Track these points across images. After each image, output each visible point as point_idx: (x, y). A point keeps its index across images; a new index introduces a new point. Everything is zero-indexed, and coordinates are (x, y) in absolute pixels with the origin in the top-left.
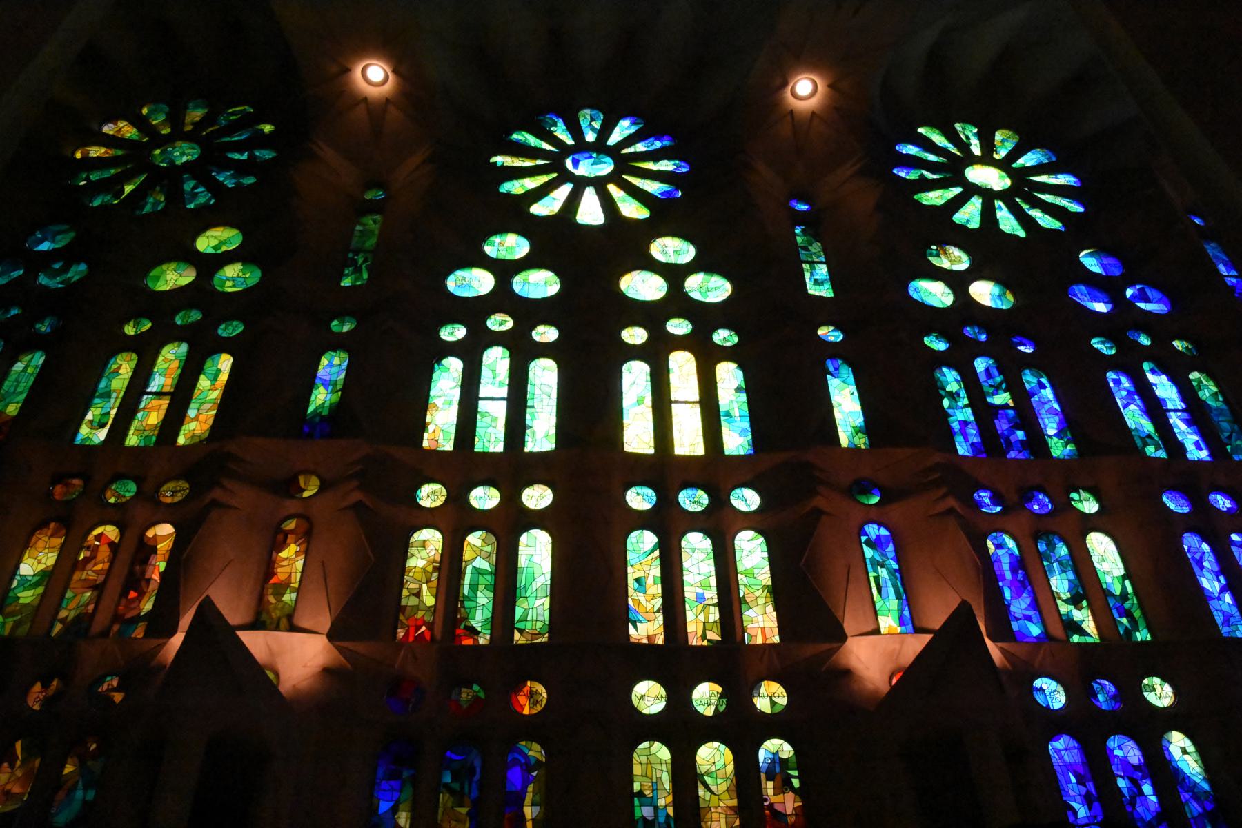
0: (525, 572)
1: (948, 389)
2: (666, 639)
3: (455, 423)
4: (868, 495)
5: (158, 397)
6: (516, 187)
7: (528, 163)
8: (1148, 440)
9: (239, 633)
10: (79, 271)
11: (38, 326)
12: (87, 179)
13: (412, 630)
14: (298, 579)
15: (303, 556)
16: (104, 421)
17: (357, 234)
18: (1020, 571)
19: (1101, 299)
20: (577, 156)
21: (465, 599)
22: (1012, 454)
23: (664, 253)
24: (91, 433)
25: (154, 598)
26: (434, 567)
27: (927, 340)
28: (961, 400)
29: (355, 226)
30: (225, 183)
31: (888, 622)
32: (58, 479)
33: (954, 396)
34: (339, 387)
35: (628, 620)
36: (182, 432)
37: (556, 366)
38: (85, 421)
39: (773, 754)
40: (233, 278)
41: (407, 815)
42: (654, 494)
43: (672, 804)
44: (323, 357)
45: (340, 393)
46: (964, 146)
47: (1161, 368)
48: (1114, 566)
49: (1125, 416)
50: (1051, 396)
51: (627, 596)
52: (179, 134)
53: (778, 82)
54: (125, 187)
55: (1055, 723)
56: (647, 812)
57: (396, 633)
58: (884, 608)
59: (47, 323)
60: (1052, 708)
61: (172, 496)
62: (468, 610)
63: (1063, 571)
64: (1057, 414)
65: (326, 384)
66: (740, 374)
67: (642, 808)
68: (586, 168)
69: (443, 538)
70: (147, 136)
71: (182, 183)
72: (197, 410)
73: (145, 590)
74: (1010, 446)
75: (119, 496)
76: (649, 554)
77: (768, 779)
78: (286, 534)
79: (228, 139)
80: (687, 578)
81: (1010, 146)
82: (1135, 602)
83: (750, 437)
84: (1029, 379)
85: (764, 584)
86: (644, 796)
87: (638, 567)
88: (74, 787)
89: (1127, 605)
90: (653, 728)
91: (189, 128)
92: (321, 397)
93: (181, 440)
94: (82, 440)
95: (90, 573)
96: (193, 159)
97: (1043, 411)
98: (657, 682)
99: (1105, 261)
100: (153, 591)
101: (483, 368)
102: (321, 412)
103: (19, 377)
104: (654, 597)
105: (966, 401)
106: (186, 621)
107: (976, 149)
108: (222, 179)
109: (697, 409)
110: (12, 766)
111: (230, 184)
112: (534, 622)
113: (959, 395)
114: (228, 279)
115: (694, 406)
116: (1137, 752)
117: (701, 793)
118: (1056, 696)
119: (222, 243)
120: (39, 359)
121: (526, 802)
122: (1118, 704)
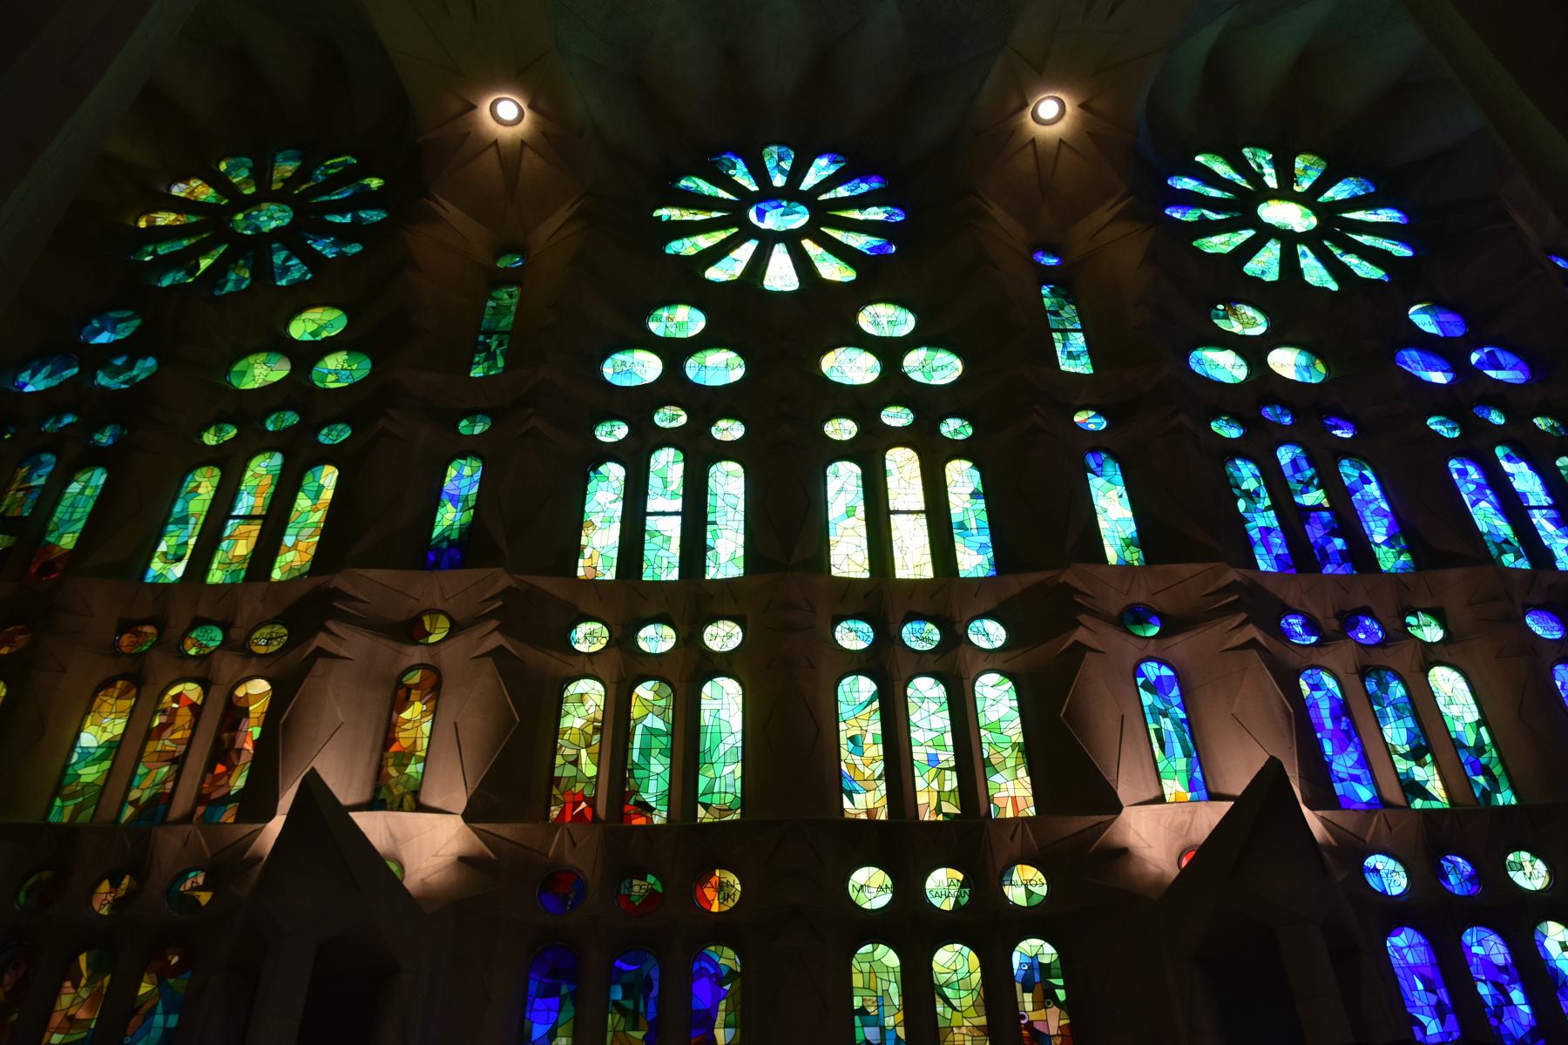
0: (709, 731)
1: (1244, 486)
2: (890, 814)
3: (617, 545)
4: (1145, 625)
5: (246, 522)
6: (687, 247)
7: (701, 216)
8: (1505, 546)
9: (352, 815)
10: (146, 366)
11: (97, 437)
12: (154, 253)
13: (568, 810)
14: (425, 746)
15: (431, 717)
16: (180, 552)
17: (489, 311)
18: (1343, 719)
19: (1438, 368)
20: (762, 206)
21: (635, 766)
22: (1329, 569)
23: (876, 324)
24: (165, 569)
25: (245, 774)
26: (595, 728)
27: (1214, 426)
28: (1262, 500)
29: (487, 301)
30: (324, 253)
31: (1175, 787)
32: (127, 626)
33: (1251, 496)
34: (471, 503)
35: (841, 791)
36: (277, 565)
37: (742, 470)
38: (157, 554)
39: (1031, 957)
40: (336, 370)
41: (567, 1041)
42: (870, 630)
43: (902, 1024)
44: (450, 467)
45: (472, 511)
46: (1256, 177)
47: (1521, 452)
48: (1466, 709)
49: (1474, 516)
50: (1377, 493)
51: (839, 760)
52: (265, 195)
53: (1015, 103)
54: (201, 261)
55: (1395, 913)
56: (872, 1033)
57: (548, 811)
58: (1169, 769)
59: (108, 432)
60: (1390, 894)
61: (267, 644)
62: (639, 781)
63: (1399, 718)
64: (1386, 516)
65: (454, 500)
66: (976, 474)
67: (865, 1028)
68: (774, 220)
69: (606, 691)
70: (226, 198)
71: (271, 253)
72: (294, 537)
73: (235, 763)
74: (1325, 558)
75: (201, 646)
76: (867, 706)
77: (1025, 990)
78: (409, 689)
79: (326, 198)
80: (916, 735)
81: (1314, 175)
82: (1494, 754)
83: (991, 555)
84: (1348, 471)
85: (1013, 741)
86: (868, 1013)
87: (853, 722)
88: (152, 1012)
89: (1484, 760)
90: (876, 927)
91: (277, 186)
92: (448, 517)
93: (276, 575)
94: (155, 577)
95: (167, 742)
96: (285, 224)
97: (1367, 513)
98: (880, 869)
99: (1442, 318)
100: (246, 763)
101: (651, 475)
102: (449, 536)
103: (75, 498)
104: (874, 760)
105: (1268, 502)
106: (286, 801)
107: (1271, 181)
108: (319, 248)
109: (922, 520)
110: (76, 986)
111: (330, 253)
112: (723, 795)
113: (1258, 495)
114: (330, 372)
115: (918, 517)
116: (1502, 949)
117: (939, 1009)
118: (1395, 878)
119: (322, 327)
120: (99, 477)
121: (717, 1023)
122: (1476, 887)
